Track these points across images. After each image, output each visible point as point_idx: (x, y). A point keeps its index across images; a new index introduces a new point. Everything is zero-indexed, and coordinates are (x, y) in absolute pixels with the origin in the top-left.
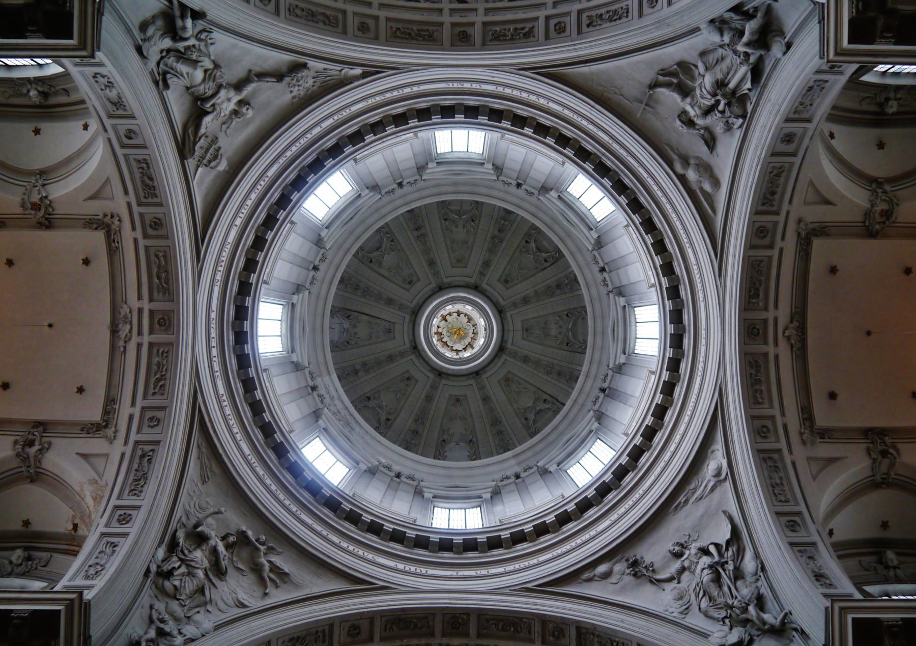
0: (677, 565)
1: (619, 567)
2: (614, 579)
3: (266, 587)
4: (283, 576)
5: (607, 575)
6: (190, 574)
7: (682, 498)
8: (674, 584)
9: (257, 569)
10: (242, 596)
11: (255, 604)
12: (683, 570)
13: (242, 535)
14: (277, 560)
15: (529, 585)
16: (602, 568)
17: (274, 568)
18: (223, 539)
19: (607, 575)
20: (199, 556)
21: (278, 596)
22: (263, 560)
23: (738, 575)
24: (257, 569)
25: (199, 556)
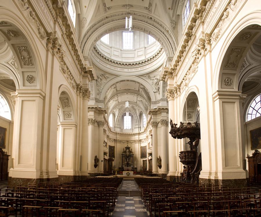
0: (153, 79)
1: (147, 76)
2: (146, 77)
3: (106, 79)
4: (108, 77)
5: (145, 76)
6: (99, 83)
7: (156, 71)
8: (152, 81)
9: (105, 78)
10: (105, 82)
11: (106, 82)
12: (153, 79)
13: (102, 75)
14: (106, 76)
15: (137, 76)
16: (145, 75)
17: (107, 77)
18: (101, 76)
19: (145, 76)
20: (99, 80)
21: (108, 80)
22: (105, 76)
23: (158, 84)
24: (105, 78)
25: (99, 80)
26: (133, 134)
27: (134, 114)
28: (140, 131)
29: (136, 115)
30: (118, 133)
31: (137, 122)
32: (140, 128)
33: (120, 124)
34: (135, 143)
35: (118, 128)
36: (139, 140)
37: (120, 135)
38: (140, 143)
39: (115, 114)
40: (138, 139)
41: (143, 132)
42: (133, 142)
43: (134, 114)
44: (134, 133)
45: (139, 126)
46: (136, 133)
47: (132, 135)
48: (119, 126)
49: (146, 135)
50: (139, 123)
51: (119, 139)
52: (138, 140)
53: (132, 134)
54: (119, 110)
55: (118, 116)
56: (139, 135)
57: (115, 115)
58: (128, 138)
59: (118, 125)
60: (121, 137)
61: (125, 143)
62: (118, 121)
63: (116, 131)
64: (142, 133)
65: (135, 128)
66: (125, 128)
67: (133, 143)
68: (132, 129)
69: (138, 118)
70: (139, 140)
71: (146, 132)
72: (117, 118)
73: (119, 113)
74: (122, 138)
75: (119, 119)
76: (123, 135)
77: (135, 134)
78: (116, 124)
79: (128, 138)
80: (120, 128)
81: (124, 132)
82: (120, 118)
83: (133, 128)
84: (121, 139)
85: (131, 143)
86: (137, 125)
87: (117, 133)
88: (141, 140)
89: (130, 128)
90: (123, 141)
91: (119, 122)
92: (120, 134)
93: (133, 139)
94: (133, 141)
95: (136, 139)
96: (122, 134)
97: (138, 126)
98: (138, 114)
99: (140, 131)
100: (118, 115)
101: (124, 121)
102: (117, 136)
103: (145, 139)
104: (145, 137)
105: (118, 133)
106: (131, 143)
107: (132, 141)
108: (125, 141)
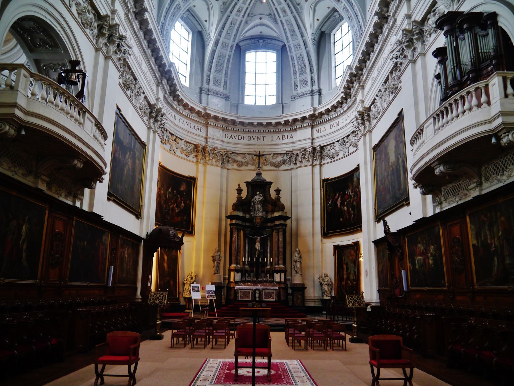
26: (286, 123)
27: (292, 31)
28: (320, 103)
29: (302, 37)
30: (213, 114)
31: (302, 72)
32: (316, 97)
33: (225, 82)
34: (292, 166)
35: (216, 94)
36: (314, 149)
37: (224, 130)
38: (315, 163)
39: (204, 33)
40: (307, 144)
41: (334, 108)
42: (284, 162)
43: (292, 31)
44: (290, 119)
45: (316, 88)
46: (299, 117)
47: (280, 128)
48: (220, 89)
49: (360, 109)
50: (312, 72)
51: (218, 144)
52: (310, 150)
53: (282, 121)
54: (223, 12)
55: (217, 43)
56: (312, 127)
57: (206, 39)
58: (261, 142)
59: (219, 85)
60: (230, 140)
61: (247, 164)
62: (219, 64)
63: (204, 105)
64: (328, 111)
65: (294, 98)
66: (249, 101)
67: (283, 167)
68: (281, 104)
69: (308, 53)
70: (314, 149)
71: (350, 101)
72: (213, 52)
73: (223, 28)
74: (236, 141)
75: (222, 56)
76: (239, 127)
77: (295, 121)
78: (209, 76)
79: (261, 142)
80: (227, 98)
81: (244, 117)
82: (228, 53)
83: (286, 101)
84: (228, 147)
85: (277, 165)
86: (305, 82)
87: (208, 116)
88: (322, 148)
89: (272, 101)
90: (239, 158)
91: (221, 71)
92: (224, 120)
93: (286, 148)
94: (286, 157)
95: (299, 146)
96: (233, 122)
97: (308, 88)
98: (310, 34)
99: (320, 103)
100: (220, 35)
101: (244, 73)
102: (210, 129)
103: (343, 141)
104: (350, 128)
105: (216, 118)
106: (273, 164)
107: (279, 159)
108: (248, 158)
